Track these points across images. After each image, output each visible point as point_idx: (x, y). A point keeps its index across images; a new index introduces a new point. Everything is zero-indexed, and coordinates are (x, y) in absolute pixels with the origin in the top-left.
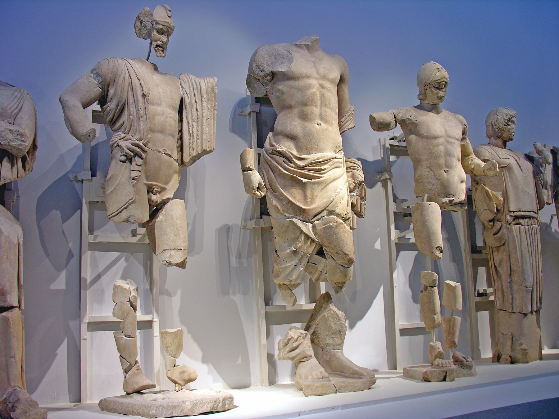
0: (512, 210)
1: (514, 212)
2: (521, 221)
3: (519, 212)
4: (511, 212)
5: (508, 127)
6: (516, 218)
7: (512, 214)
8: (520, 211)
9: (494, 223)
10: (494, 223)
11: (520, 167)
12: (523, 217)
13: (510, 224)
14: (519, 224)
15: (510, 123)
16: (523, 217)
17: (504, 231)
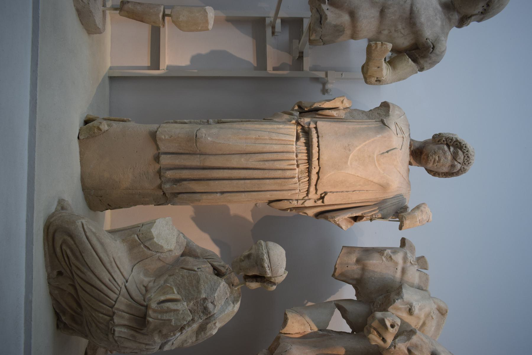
0: (320, 124)
1: (316, 128)
2: (303, 140)
3: (316, 135)
4: (316, 123)
5: (446, 148)
6: (307, 133)
7: (312, 126)
8: (318, 137)
9: (296, 110)
10: (296, 110)
11: (387, 152)
12: (308, 145)
13: (298, 124)
14: (298, 139)
15: (452, 149)
16: (308, 145)
17: (287, 117)
